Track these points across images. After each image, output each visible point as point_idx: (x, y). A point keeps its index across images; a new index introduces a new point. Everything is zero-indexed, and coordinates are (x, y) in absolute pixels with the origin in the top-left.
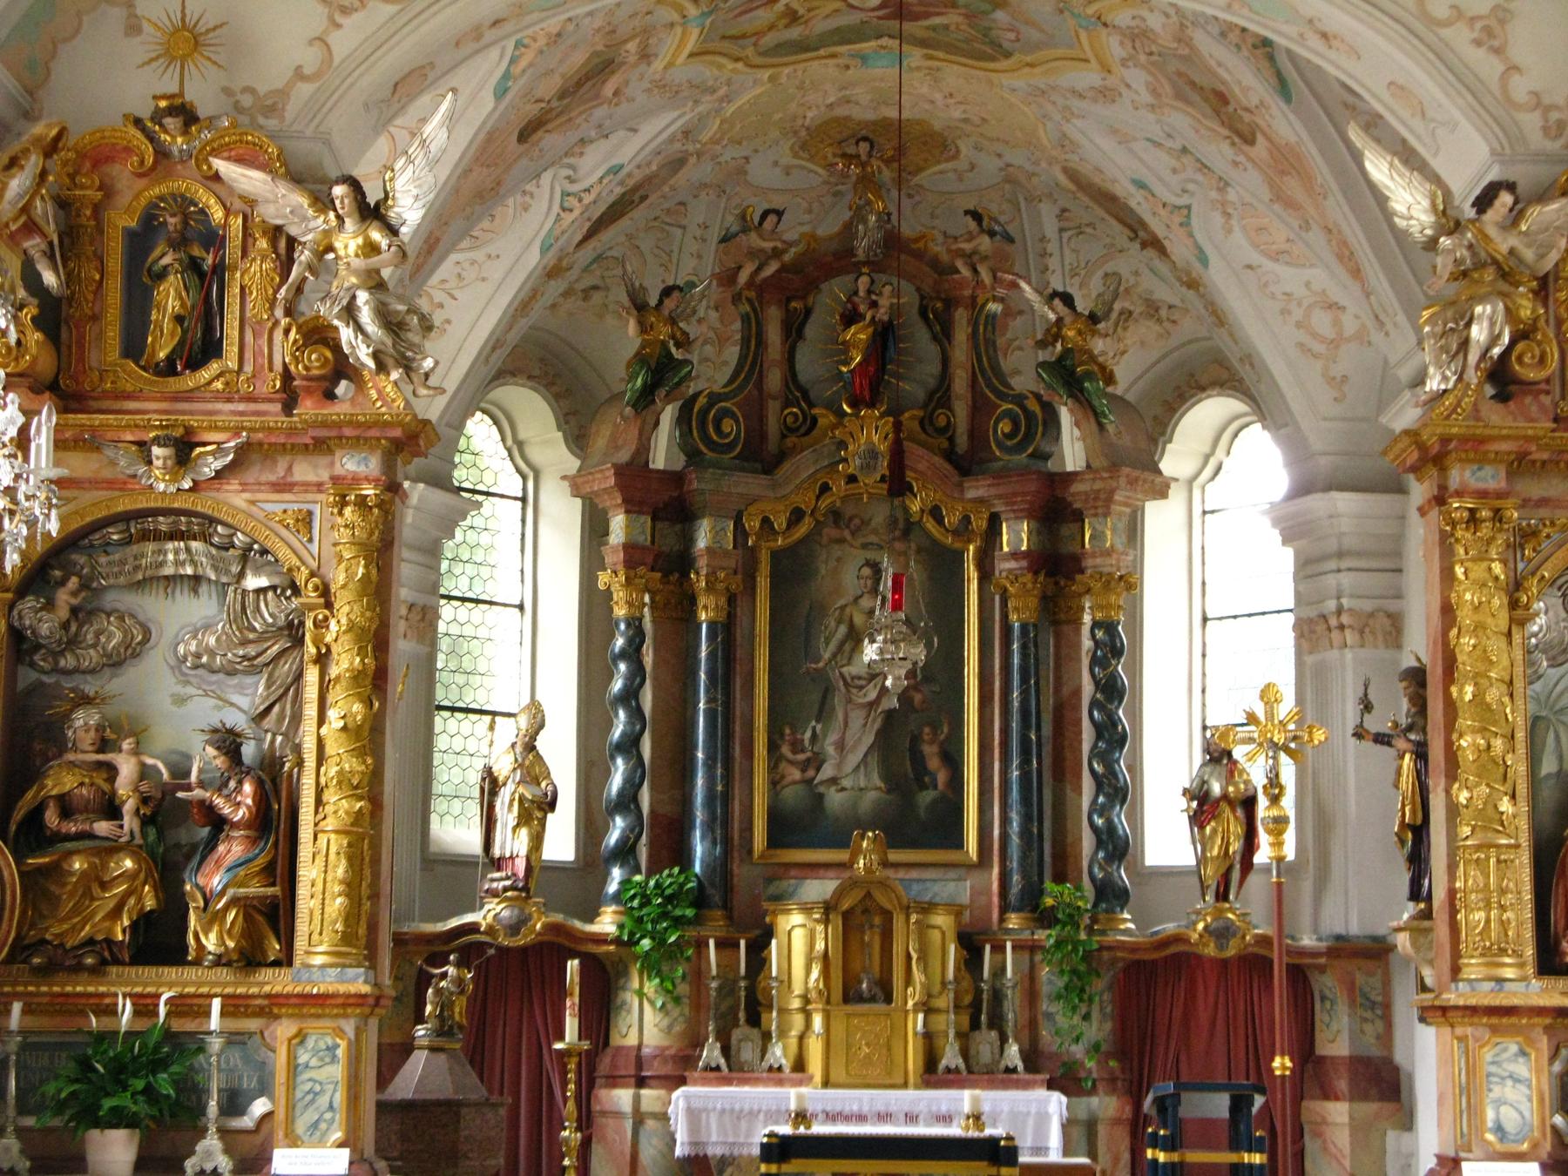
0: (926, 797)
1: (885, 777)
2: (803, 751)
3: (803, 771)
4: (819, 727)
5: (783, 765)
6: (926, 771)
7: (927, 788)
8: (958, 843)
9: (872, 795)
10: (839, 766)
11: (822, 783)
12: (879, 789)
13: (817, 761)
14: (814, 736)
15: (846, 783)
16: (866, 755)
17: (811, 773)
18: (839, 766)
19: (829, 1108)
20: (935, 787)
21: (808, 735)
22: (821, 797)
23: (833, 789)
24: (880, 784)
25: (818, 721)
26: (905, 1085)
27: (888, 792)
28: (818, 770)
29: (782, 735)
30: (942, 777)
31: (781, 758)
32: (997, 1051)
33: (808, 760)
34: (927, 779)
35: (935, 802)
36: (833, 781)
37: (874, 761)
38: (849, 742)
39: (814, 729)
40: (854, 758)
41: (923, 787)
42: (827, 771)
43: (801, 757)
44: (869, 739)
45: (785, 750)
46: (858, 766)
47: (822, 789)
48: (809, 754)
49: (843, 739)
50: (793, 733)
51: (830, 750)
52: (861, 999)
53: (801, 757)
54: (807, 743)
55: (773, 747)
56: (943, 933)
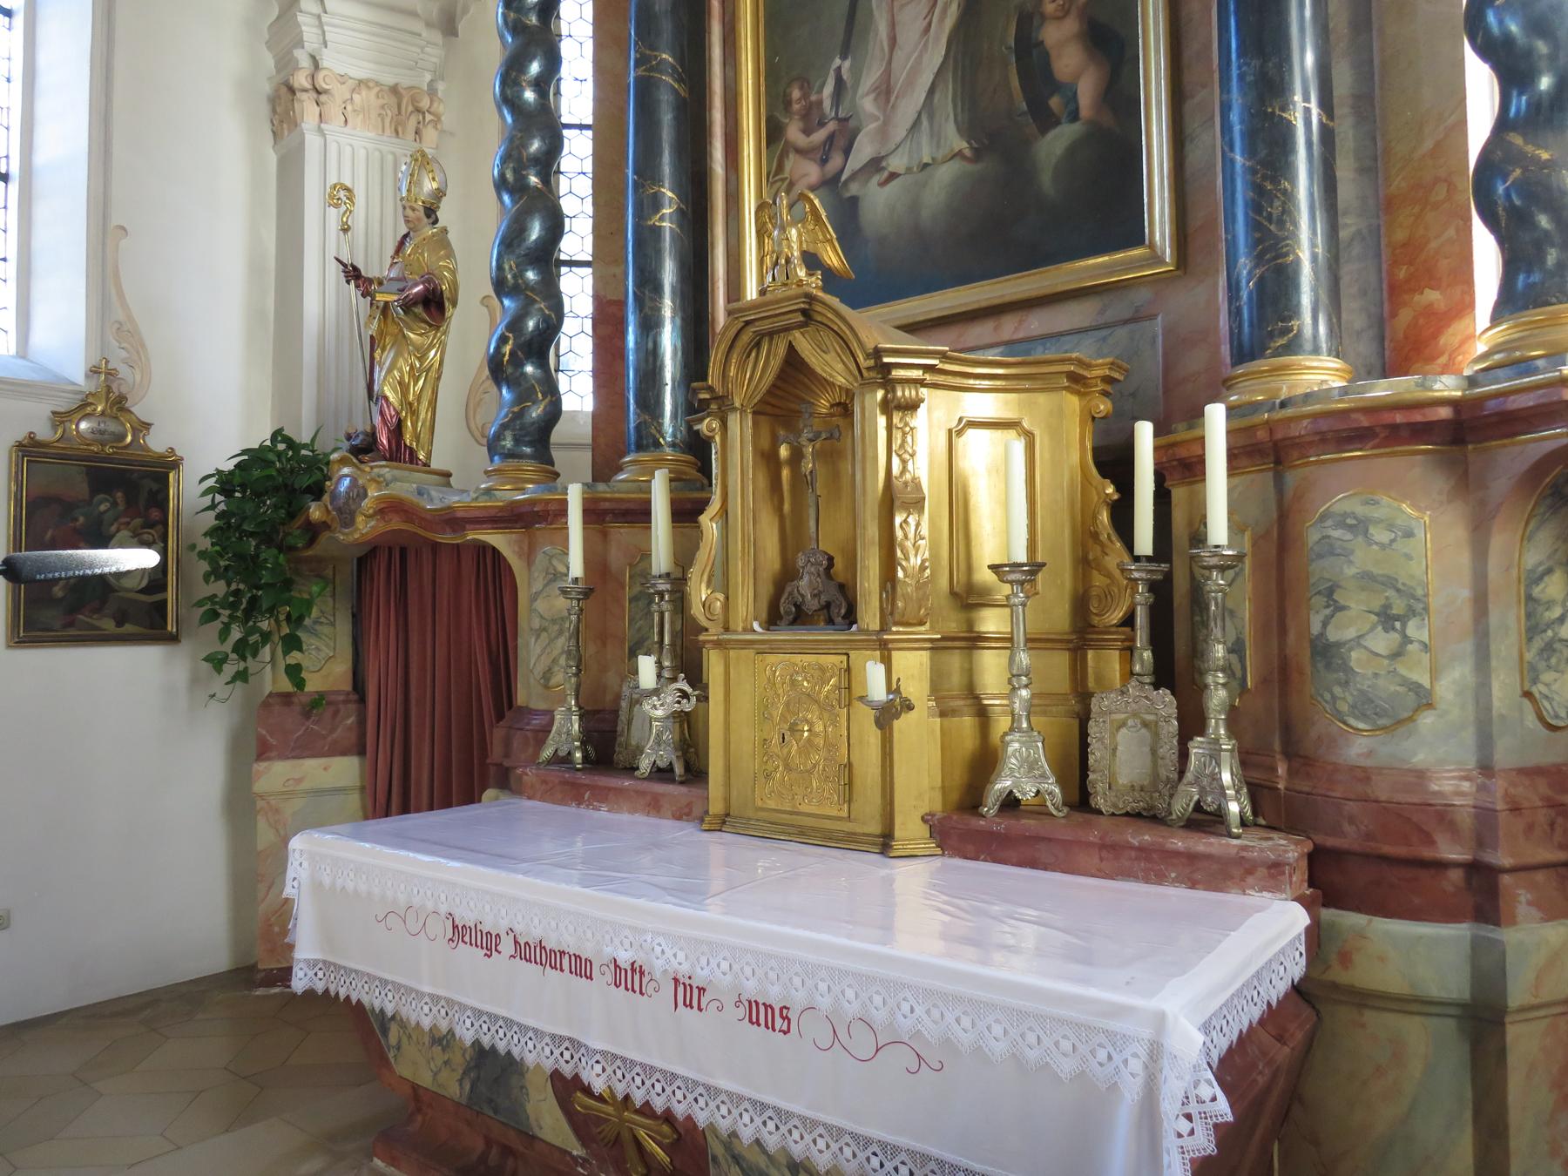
0: (1054, 145)
1: (969, 129)
2: (822, 124)
3: (824, 162)
4: (847, 64)
5: (792, 162)
6: (1054, 86)
7: (1058, 123)
8: (1132, 233)
9: (946, 174)
10: (883, 132)
11: (854, 176)
12: (960, 154)
13: (845, 139)
14: (839, 82)
15: (896, 163)
16: (931, 92)
17: (836, 161)
18: (883, 132)
19: (518, 928)
20: (1074, 116)
21: (828, 89)
22: (854, 201)
23: (876, 179)
24: (961, 144)
25: (844, 58)
26: (885, 843)
27: (978, 155)
28: (847, 152)
29: (788, 103)
30: (1087, 91)
31: (790, 148)
32: (1169, 749)
33: (831, 138)
34: (1055, 102)
35: (1072, 150)
36: (875, 164)
37: (946, 102)
38: (900, 78)
39: (839, 68)
40: (910, 105)
41: (1046, 121)
42: (864, 150)
43: (820, 136)
44: (935, 56)
45: (794, 133)
46: (916, 123)
47: (854, 189)
48: (831, 126)
49: (888, 73)
50: (805, 96)
51: (868, 105)
52: (800, 618)
53: (820, 136)
54: (827, 104)
55: (773, 133)
56: (1030, 438)
